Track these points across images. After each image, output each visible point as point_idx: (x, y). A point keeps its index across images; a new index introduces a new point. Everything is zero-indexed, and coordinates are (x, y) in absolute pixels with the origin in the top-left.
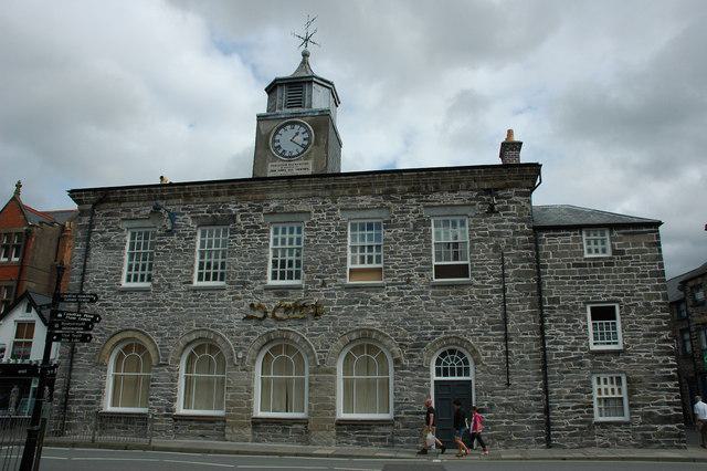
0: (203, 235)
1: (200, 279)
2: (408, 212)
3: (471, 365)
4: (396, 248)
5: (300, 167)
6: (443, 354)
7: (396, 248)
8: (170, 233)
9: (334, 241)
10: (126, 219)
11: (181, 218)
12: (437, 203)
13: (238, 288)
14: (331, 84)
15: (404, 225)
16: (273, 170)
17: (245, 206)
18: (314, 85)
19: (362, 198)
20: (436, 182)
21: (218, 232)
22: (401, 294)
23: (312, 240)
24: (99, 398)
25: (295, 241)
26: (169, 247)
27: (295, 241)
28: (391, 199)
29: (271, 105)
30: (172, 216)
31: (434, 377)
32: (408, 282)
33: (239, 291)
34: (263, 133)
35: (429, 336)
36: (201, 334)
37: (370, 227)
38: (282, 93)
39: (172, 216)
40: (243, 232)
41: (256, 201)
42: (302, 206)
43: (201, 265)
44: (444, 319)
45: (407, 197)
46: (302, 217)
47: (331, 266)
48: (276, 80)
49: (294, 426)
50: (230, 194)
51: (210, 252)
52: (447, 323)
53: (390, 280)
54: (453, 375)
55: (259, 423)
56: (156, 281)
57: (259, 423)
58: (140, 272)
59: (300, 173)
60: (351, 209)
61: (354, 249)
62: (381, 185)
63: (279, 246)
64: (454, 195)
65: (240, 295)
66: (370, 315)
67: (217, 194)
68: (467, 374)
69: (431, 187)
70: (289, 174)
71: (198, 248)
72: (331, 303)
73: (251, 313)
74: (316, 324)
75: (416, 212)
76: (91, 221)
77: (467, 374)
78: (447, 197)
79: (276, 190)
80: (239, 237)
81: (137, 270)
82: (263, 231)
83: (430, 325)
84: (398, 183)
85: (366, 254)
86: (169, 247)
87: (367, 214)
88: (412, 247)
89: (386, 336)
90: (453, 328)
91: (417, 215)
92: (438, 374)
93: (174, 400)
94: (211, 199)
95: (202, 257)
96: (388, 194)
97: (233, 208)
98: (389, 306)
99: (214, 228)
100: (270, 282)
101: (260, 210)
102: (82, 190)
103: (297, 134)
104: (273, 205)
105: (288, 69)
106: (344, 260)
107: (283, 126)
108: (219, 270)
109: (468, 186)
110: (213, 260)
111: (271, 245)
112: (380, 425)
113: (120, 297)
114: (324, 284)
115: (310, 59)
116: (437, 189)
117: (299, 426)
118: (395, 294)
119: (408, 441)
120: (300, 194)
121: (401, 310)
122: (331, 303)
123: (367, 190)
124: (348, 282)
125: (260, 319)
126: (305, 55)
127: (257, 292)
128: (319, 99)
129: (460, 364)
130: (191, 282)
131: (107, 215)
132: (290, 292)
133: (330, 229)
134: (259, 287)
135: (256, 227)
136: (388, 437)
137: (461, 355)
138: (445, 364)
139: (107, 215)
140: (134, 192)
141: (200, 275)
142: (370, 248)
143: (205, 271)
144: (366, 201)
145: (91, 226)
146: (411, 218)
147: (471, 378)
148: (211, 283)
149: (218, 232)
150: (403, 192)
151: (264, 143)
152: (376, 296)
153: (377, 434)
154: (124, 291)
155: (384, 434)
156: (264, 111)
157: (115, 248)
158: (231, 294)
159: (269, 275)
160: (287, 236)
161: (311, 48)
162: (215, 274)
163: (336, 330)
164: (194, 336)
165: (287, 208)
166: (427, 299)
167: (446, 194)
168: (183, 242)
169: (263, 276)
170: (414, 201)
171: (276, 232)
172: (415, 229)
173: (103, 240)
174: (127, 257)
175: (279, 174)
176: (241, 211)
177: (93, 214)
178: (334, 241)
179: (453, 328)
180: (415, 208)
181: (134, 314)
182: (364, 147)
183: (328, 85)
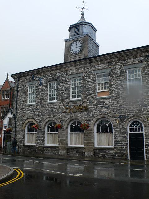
0: (50, 85)
1: (50, 100)
2: (118, 69)
3: (143, 127)
4: (114, 83)
5: (79, 57)
6: (133, 123)
7: (114, 83)
8: (40, 85)
9: (91, 83)
10: (27, 82)
11: (43, 80)
12: (128, 64)
13: (61, 102)
14: (90, 23)
15: (116, 74)
16: (71, 59)
17: (62, 73)
18: (83, 25)
19: (101, 65)
20: (127, 55)
21: (54, 83)
22: (115, 100)
23: (84, 83)
24: (23, 141)
25: (76, 84)
26: (40, 90)
27: (76, 84)
28: (111, 64)
29: (71, 35)
30: (40, 79)
31: (129, 132)
32: (118, 95)
33: (61, 103)
34: (67, 46)
35: (126, 116)
36: (50, 119)
37: (104, 76)
38: (73, 30)
39: (40, 79)
40: (62, 82)
41: (65, 71)
42: (81, 71)
43: (50, 95)
44: (131, 109)
45: (117, 63)
46: (81, 74)
47: (91, 92)
48: (70, 26)
49: (80, 150)
50: (57, 69)
51: (52, 90)
52: (133, 111)
53: (111, 95)
54: (136, 131)
55: (69, 149)
56: (37, 102)
57: (69, 149)
58: (32, 99)
59: (79, 59)
60: (98, 70)
61: (99, 84)
62: (107, 59)
63: (74, 86)
64: (135, 60)
65: (62, 104)
66: (104, 109)
67: (53, 70)
68: (142, 130)
69: (126, 58)
70: (76, 59)
71: (49, 90)
72: (91, 105)
73: (65, 110)
74: (86, 113)
75: (121, 68)
76: (18, 84)
77: (142, 130)
78: (132, 61)
79: (71, 66)
80: (61, 84)
81: (52, 96)
82: (68, 81)
83: (127, 112)
84: (113, 58)
85: (103, 86)
86: (40, 90)
87: (104, 71)
88: (119, 82)
89: (111, 116)
90: (136, 112)
91: (121, 69)
92: (131, 131)
93: (44, 141)
94: (51, 72)
95: (50, 92)
96: (110, 63)
97: (58, 74)
98: (111, 105)
99: (53, 82)
100: (72, 99)
101: (67, 74)
102: (17, 74)
103: (77, 44)
104: (71, 71)
105: (76, 20)
106: (96, 89)
107: (73, 43)
108: (77, 94)
109: (140, 55)
110: (53, 93)
111: (71, 86)
112: (109, 150)
113: (27, 108)
114: (88, 99)
115: (85, 16)
116: (128, 58)
117: (82, 150)
118: (113, 100)
119: (119, 156)
120: (79, 67)
121: (116, 106)
122: (91, 105)
123: (102, 62)
124: (97, 97)
125: (68, 113)
126: (83, 14)
127: (66, 103)
128: (85, 30)
129: (139, 126)
130: (47, 101)
131: (22, 81)
132: (78, 102)
133: (90, 78)
134: (67, 101)
135: (66, 80)
136: (112, 154)
137: (139, 123)
138: (133, 127)
139: (22, 81)
140: (28, 73)
141: (50, 99)
142: (105, 83)
143: (74, 94)
144: (102, 66)
145: (18, 85)
146: (119, 71)
147: (143, 132)
148: (53, 101)
149: (54, 83)
150: (115, 61)
151: (68, 49)
152: (106, 102)
153: (108, 153)
154: (28, 106)
155: (111, 153)
156: (68, 37)
157: (25, 92)
158: (59, 104)
159: (71, 97)
160: (76, 82)
161: (84, 11)
162: (75, 96)
163: (93, 115)
164: (48, 120)
165: (76, 72)
166: (125, 101)
167: (132, 60)
168: (44, 88)
169: (69, 97)
170: (119, 64)
171: (73, 82)
172: (120, 75)
173: (22, 90)
174: (28, 95)
175: (72, 60)
176: (61, 75)
177: (18, 82)
178: (91, 83)
179: (136, 112)
180: (120, 66)
181: (31, 113)
182: (107, 44)
183: (89, 24)
